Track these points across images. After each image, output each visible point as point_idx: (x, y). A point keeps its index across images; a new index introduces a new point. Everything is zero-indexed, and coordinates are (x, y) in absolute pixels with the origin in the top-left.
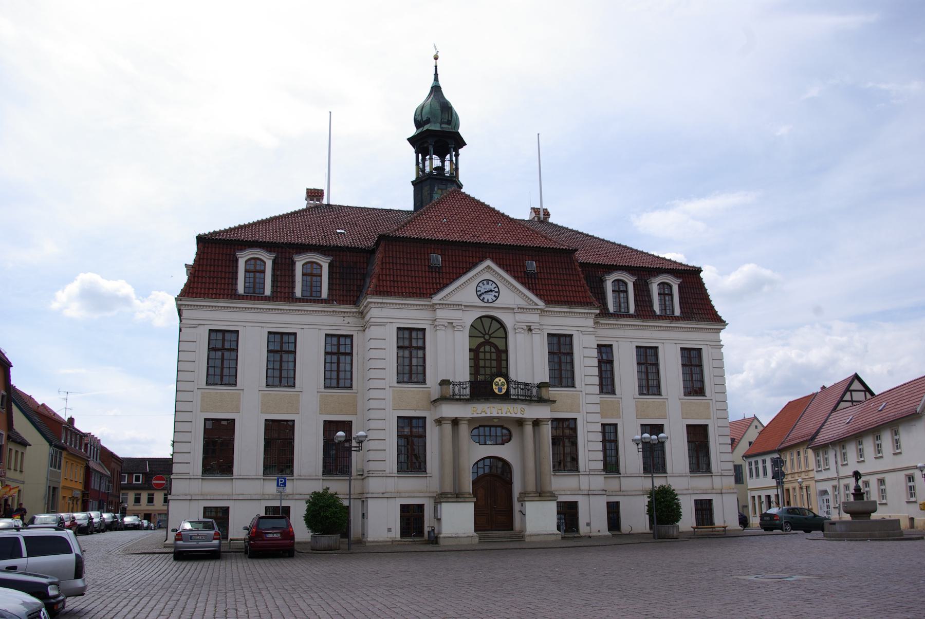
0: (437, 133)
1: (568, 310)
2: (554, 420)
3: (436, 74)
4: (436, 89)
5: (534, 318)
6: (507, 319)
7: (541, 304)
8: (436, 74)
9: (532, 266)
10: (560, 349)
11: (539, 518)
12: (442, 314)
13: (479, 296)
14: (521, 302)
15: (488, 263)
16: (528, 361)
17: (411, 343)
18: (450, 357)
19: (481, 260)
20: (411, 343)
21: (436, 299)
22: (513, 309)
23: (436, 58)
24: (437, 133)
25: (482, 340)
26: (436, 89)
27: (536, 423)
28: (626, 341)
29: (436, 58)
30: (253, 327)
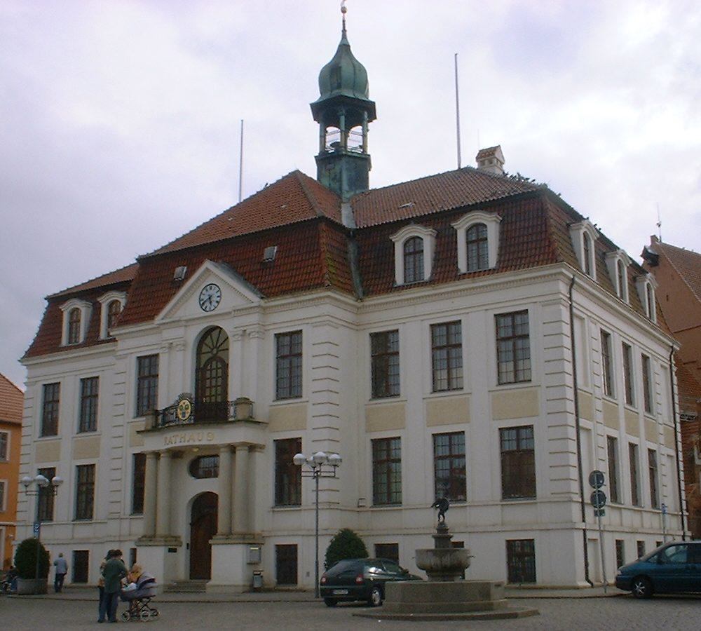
0: (343, 100)
1: (293, 300)
2: (168, 450)
3: (344, 31)
4: (344, 48)
5: (254, 318)
6: (227, 326)
7: (255, 299)
8: (344, 31)
9: (271, 252)
10: (289, 349)
11: (228, 563)
12: (168, 334)
13: (202, 305)
14: (239, 303)
15: (208, 264)
16: (250, 373)
17: (148, 369)
18: (177, 381)
19: (201, 262)
20: (148, 369)
21: (158, 320)
22: (230, 313)
23: (344, 11)
24: (343, 100)
25: (210, 355)
26: (344, 48)
27: (232, 449)
28: (411, 319)
29: (344, 11)
30: (68, 372)
